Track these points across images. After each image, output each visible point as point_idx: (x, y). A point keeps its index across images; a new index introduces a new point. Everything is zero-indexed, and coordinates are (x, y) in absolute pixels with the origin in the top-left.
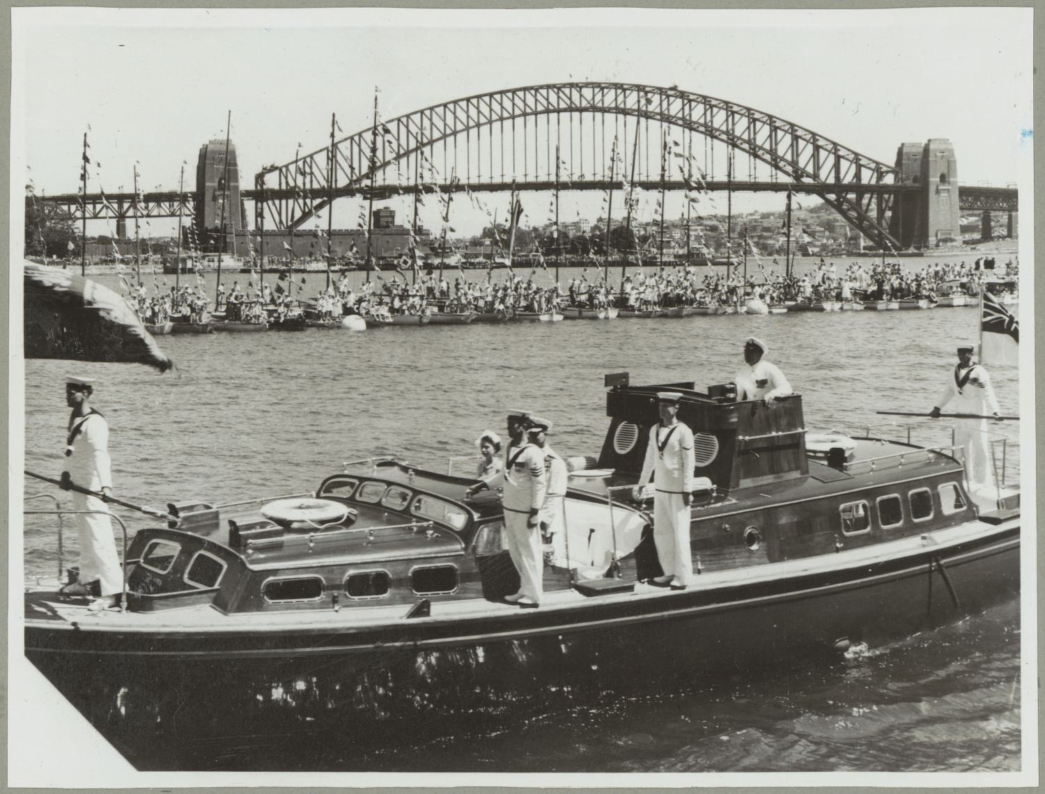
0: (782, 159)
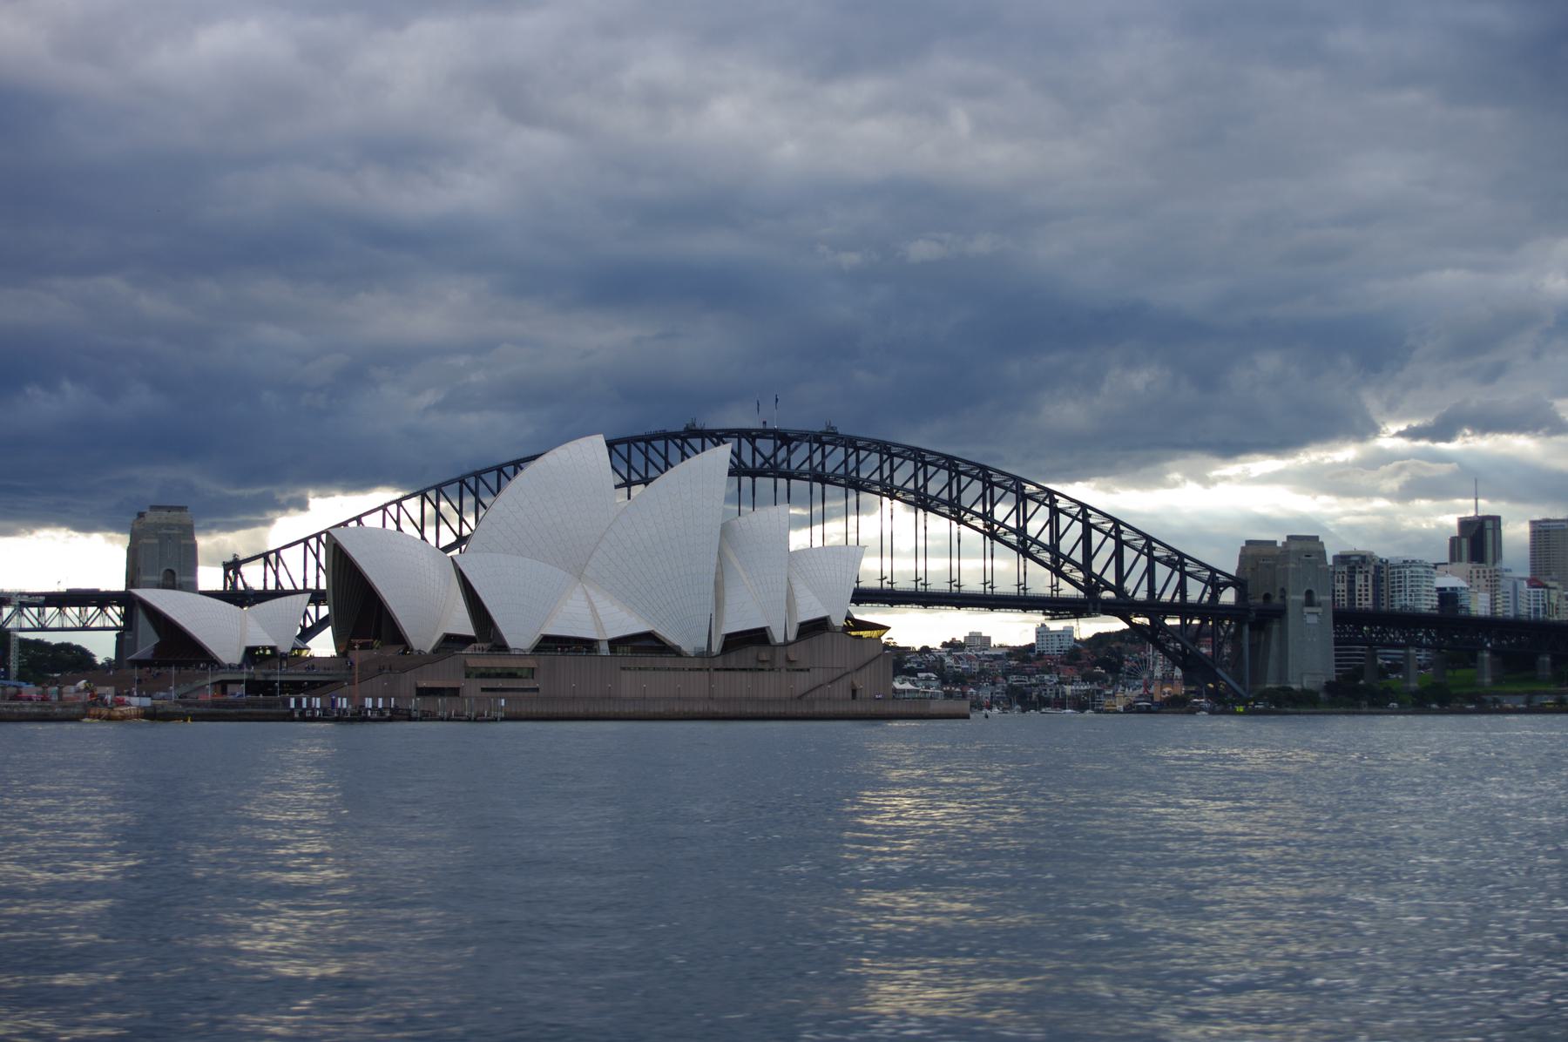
0: (1068, 559)
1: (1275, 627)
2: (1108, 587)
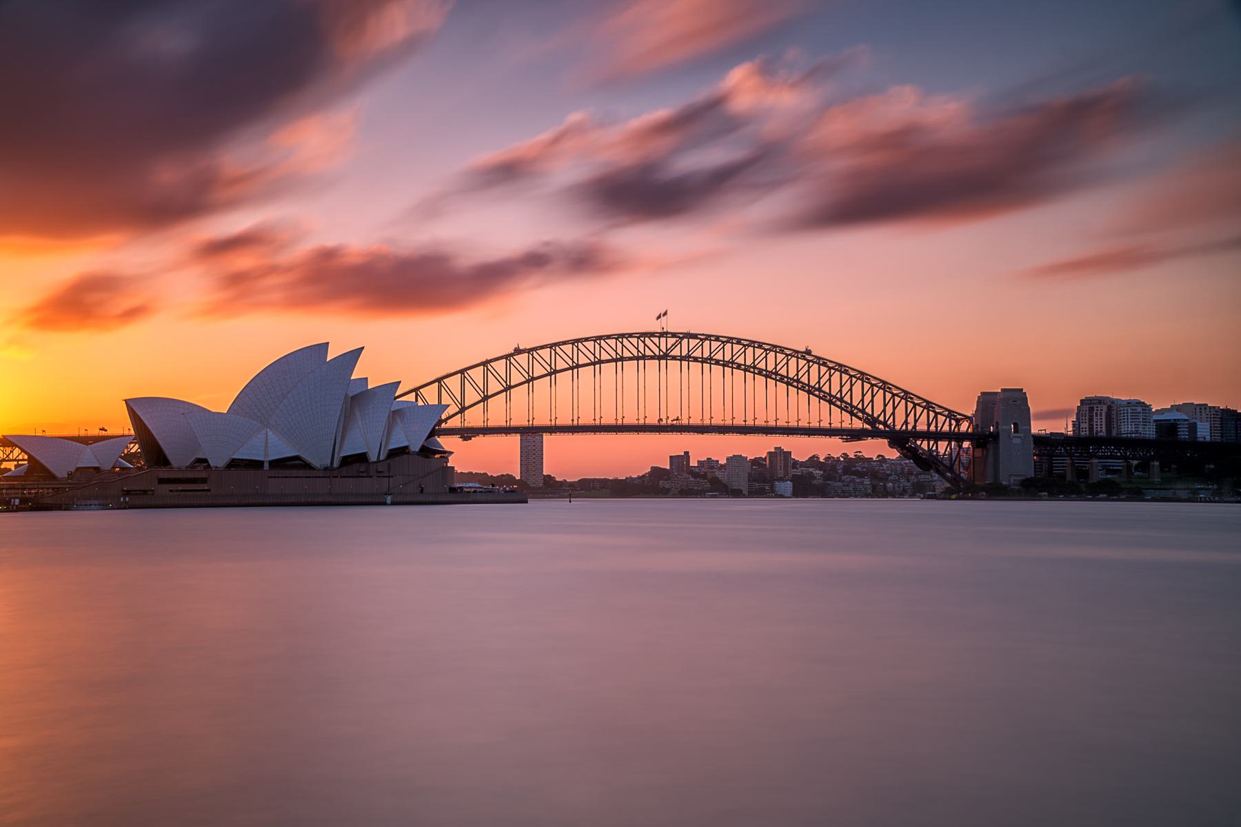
1: (991, 447)
2: (880, 423)
